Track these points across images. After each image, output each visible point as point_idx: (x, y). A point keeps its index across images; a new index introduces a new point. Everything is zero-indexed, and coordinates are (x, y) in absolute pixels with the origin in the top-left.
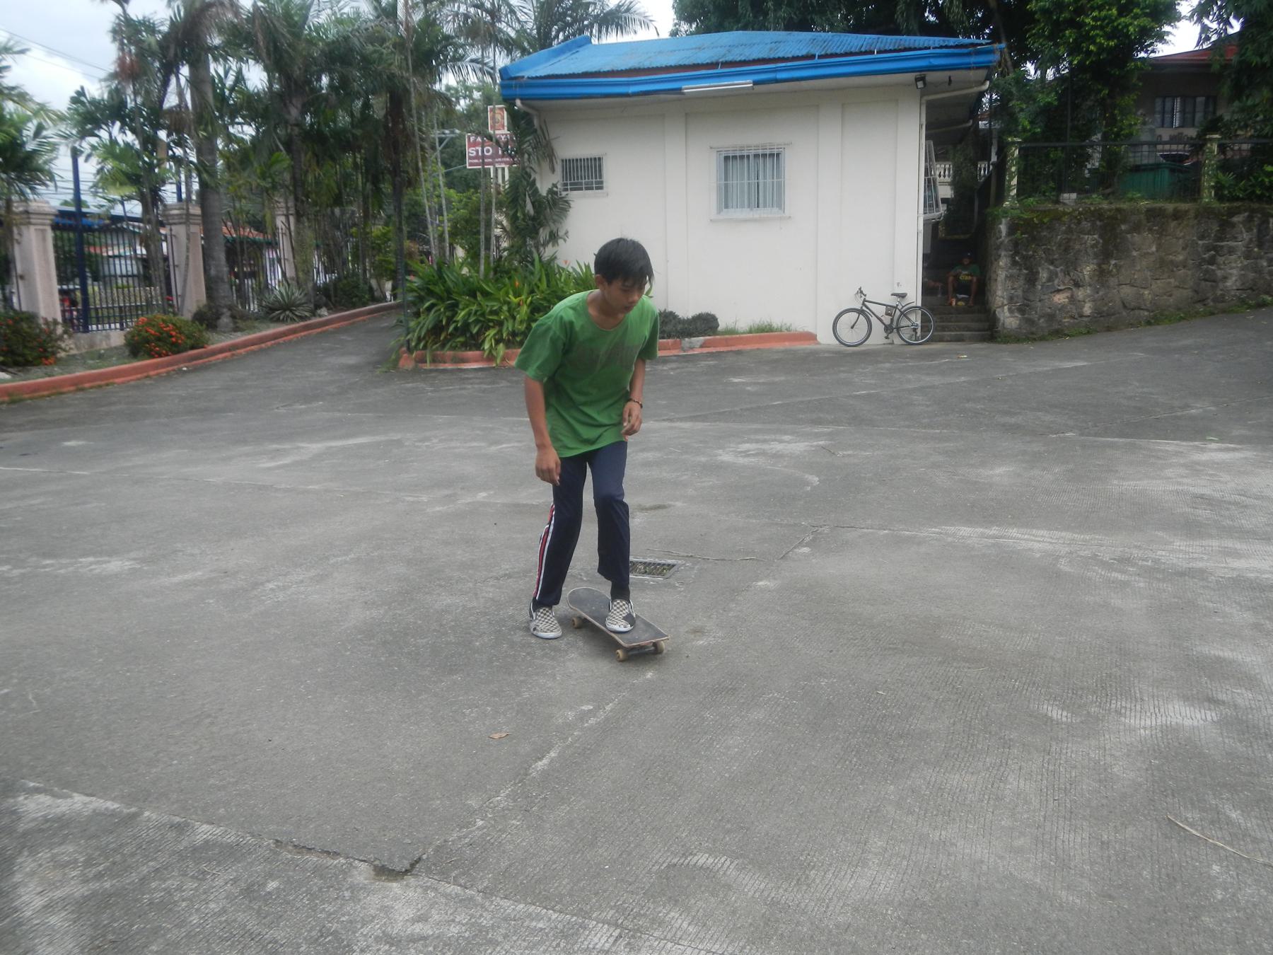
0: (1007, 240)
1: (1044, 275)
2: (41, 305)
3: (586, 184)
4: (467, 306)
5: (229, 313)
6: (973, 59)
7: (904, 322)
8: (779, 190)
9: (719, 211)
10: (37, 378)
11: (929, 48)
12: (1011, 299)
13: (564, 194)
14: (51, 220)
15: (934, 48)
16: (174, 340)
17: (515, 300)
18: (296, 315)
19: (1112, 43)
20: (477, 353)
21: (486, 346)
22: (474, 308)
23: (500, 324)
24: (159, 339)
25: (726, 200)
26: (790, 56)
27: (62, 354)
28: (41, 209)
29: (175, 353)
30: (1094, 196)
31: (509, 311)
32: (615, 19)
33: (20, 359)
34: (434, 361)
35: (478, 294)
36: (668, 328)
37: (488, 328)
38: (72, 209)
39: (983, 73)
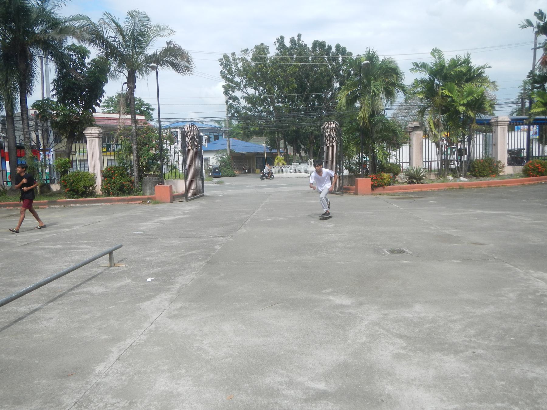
16: (540, 170)
24: (534, 170)
27: (501, 174)
28: (503, 120)
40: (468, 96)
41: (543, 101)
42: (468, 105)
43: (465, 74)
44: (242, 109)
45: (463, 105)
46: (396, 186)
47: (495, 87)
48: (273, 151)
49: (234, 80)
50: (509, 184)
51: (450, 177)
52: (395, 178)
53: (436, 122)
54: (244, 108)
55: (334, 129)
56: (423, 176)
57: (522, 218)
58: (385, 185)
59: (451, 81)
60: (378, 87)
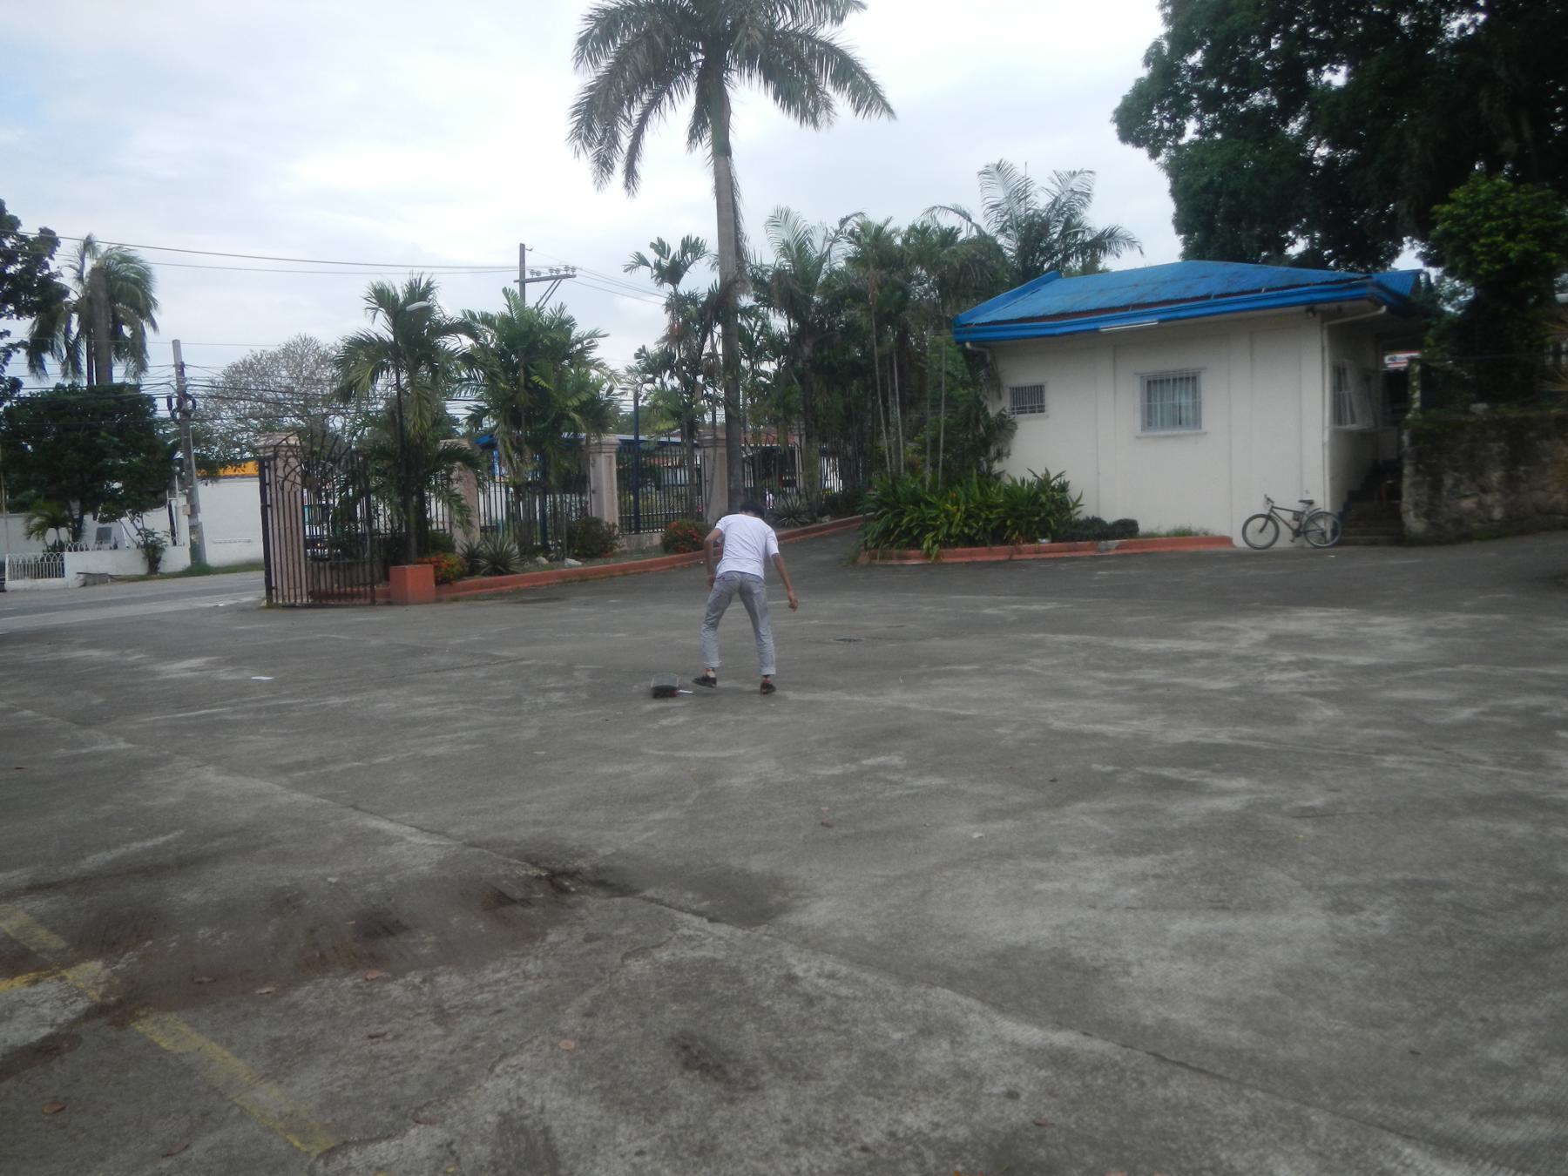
0: (1409, 450)
1: (1448, 482)
2: (605, 513)
3: (1031, 408)
6: (1347, 293)
7: (1312, 527)
8: (1197, 408)
9: (1143, 430)
10: (599, 565)
11: (1308, 285)
12: (1416, 505)
13: (1012, 417)
15: (1314, 285)
17: (955, 507)
19: (1498, 267)
20: (919, 551)
21: (925, 546)
22: (916, 515)
23: (936, 528)
25: (1150, 420)
26: (1190, 296)
27: (618, 550)
29: (695, 550)
30: (1502, 405)
31: (946, 517)
32: (1104, 242)
33: (589, 553)
34: (882, 558)
35: (922, 505)
36: (1087, 533)
37: (928, 532)
38: (632, 437)
39: (1366, 303)
45: (575, 409)
51: (543, 560)
53: (515, 443)
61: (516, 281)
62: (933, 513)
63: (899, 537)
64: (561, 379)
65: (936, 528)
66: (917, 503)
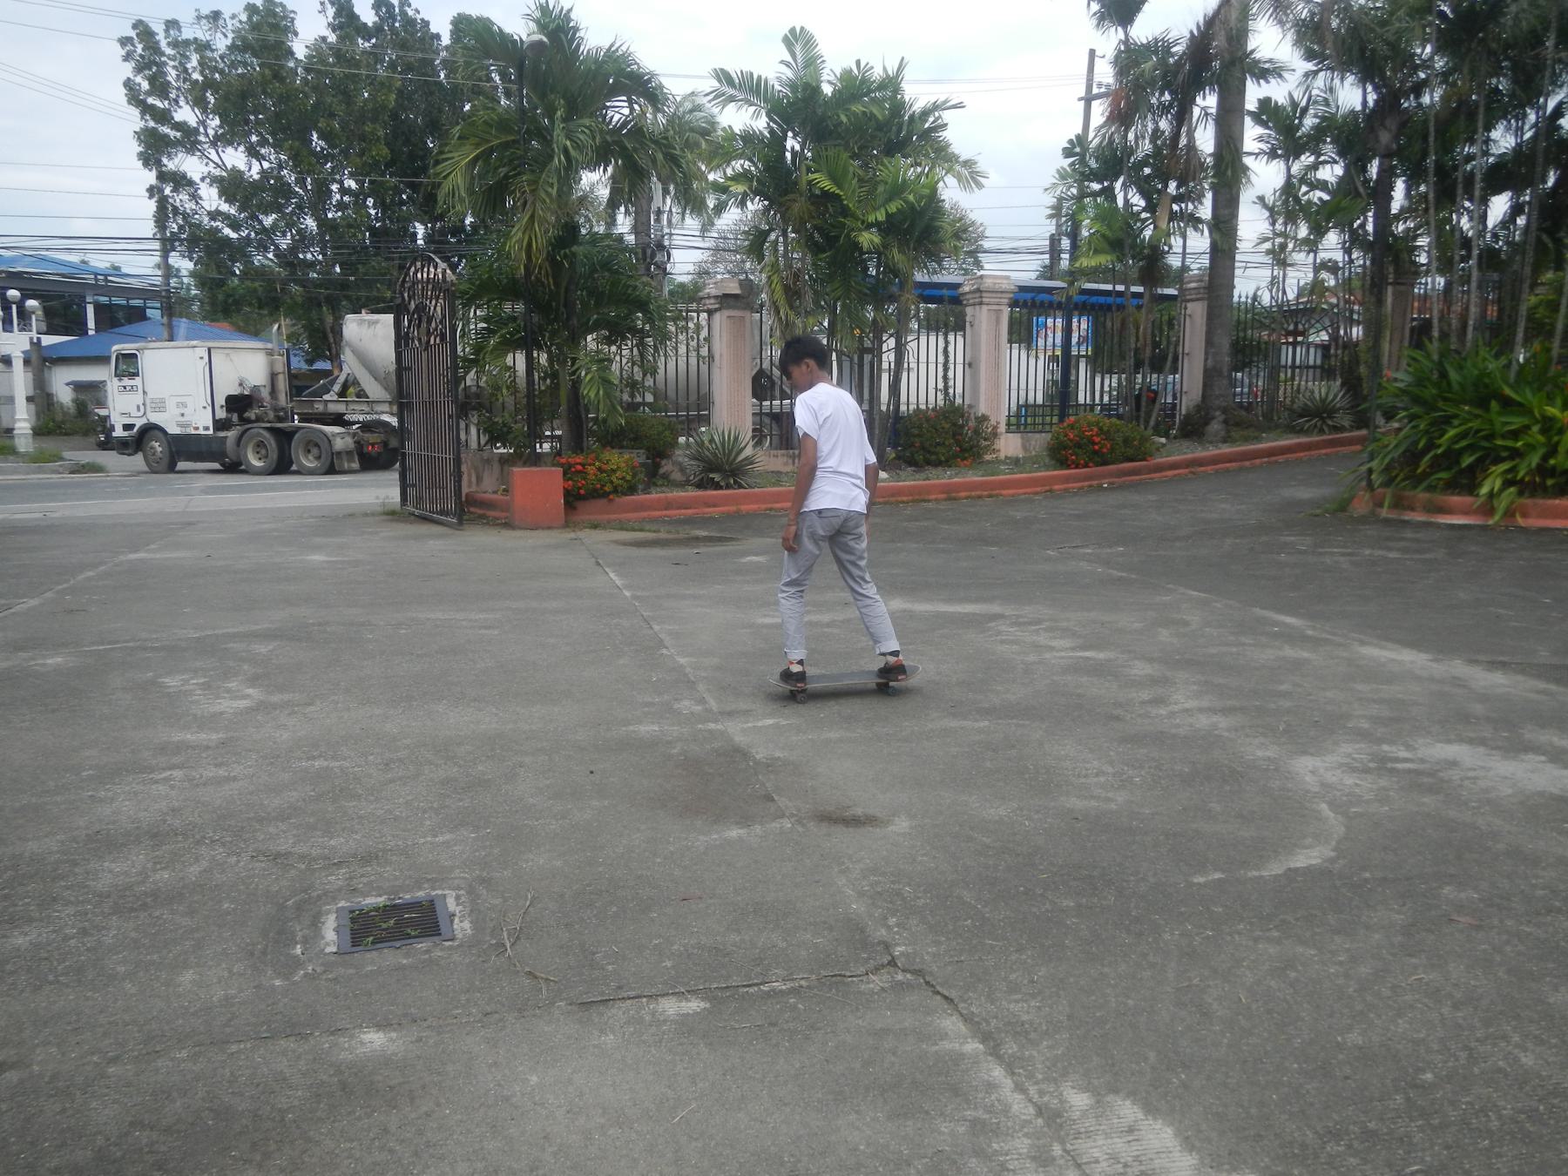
2: (982, 398)
4: (1466, 421)
5: (1222, 418)
14: (1010, 299)
16: (1096, 447)
18: (1328, 425)
20: (1468, 499)
21: (1484, 490)
22: (1475, 424)
23: (1515, 454)
24: (1079, 446)
27: (988, 457)
28: (997, 286)
31: (1544, 431)
34: (1398, 504)
35: (1494, 405)
37: (1498, 460)
40: (890, 200)
41: (1108, 233)
42: (889, 228)
43: (881, 127)
44: (206, 220)
46: (654, 495)
47: (972, 178)
48: (321, 365)
49: (174, 114)
50: (1011, 492)
52: (657, 466)
54: (214, 215)
55: (430, 287)
56: (749, 461)
57: (1042, 639)
58: (615, 491)
59: (839, 145)
60: (581, 137)
61: (1080, 99)
62: (1516, 422)
63: (1436, 465)
64: (870, 183)
65: (1515, 454)
66: (1483, 403)
